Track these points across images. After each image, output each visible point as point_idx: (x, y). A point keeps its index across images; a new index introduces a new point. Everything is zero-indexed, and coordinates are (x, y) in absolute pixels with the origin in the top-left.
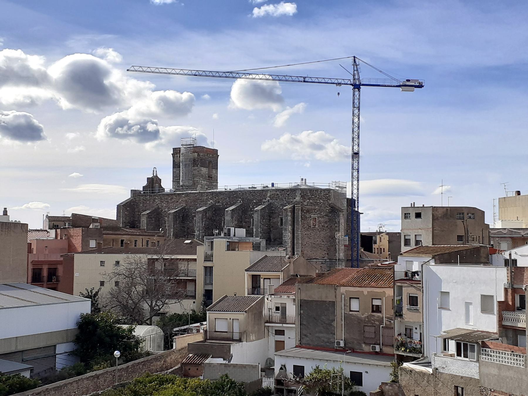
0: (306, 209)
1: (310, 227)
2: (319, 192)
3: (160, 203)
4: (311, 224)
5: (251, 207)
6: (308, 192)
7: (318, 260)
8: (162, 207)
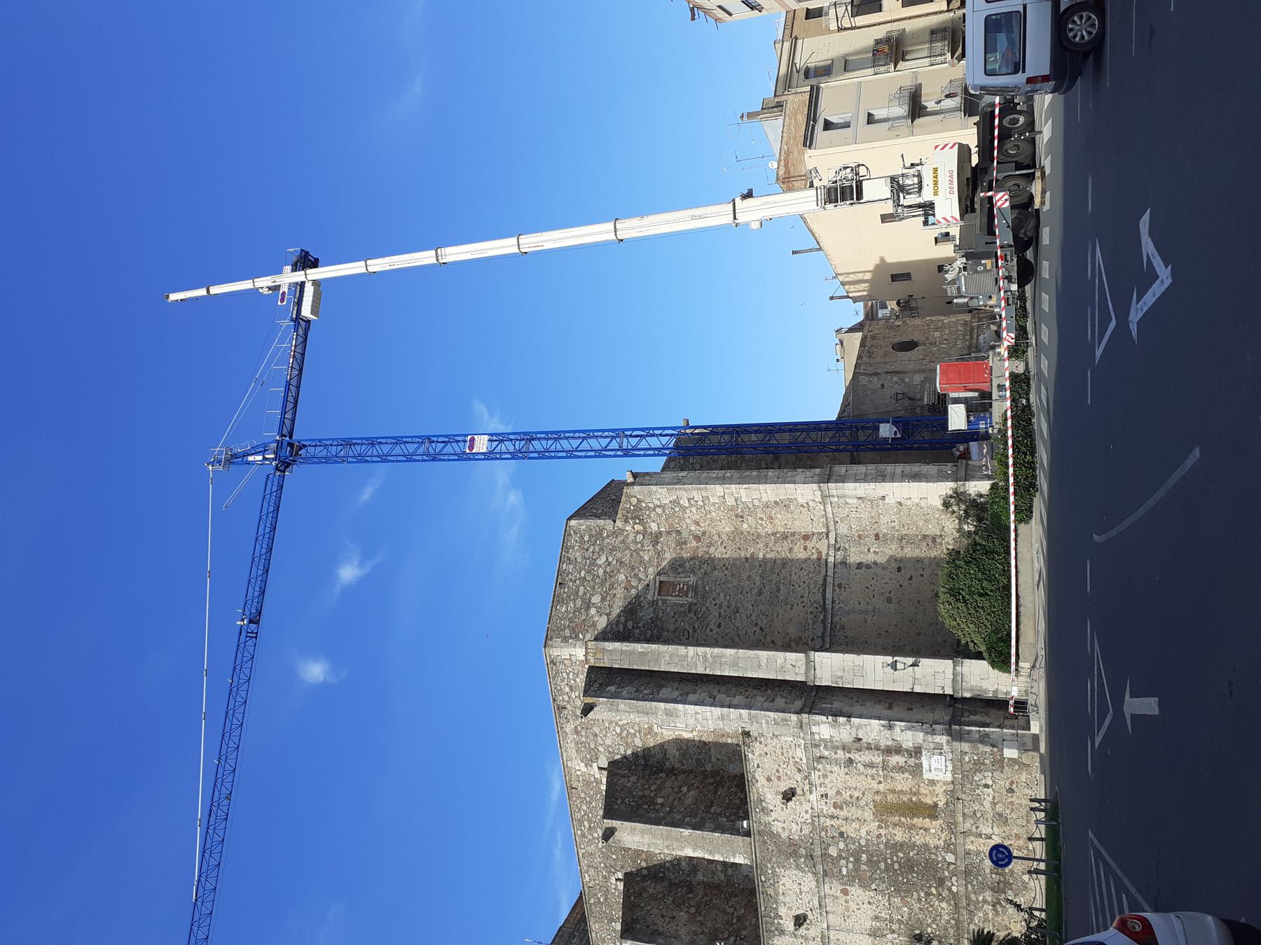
1: (691, 605)
2: (571, 567)
7: (830, 580)
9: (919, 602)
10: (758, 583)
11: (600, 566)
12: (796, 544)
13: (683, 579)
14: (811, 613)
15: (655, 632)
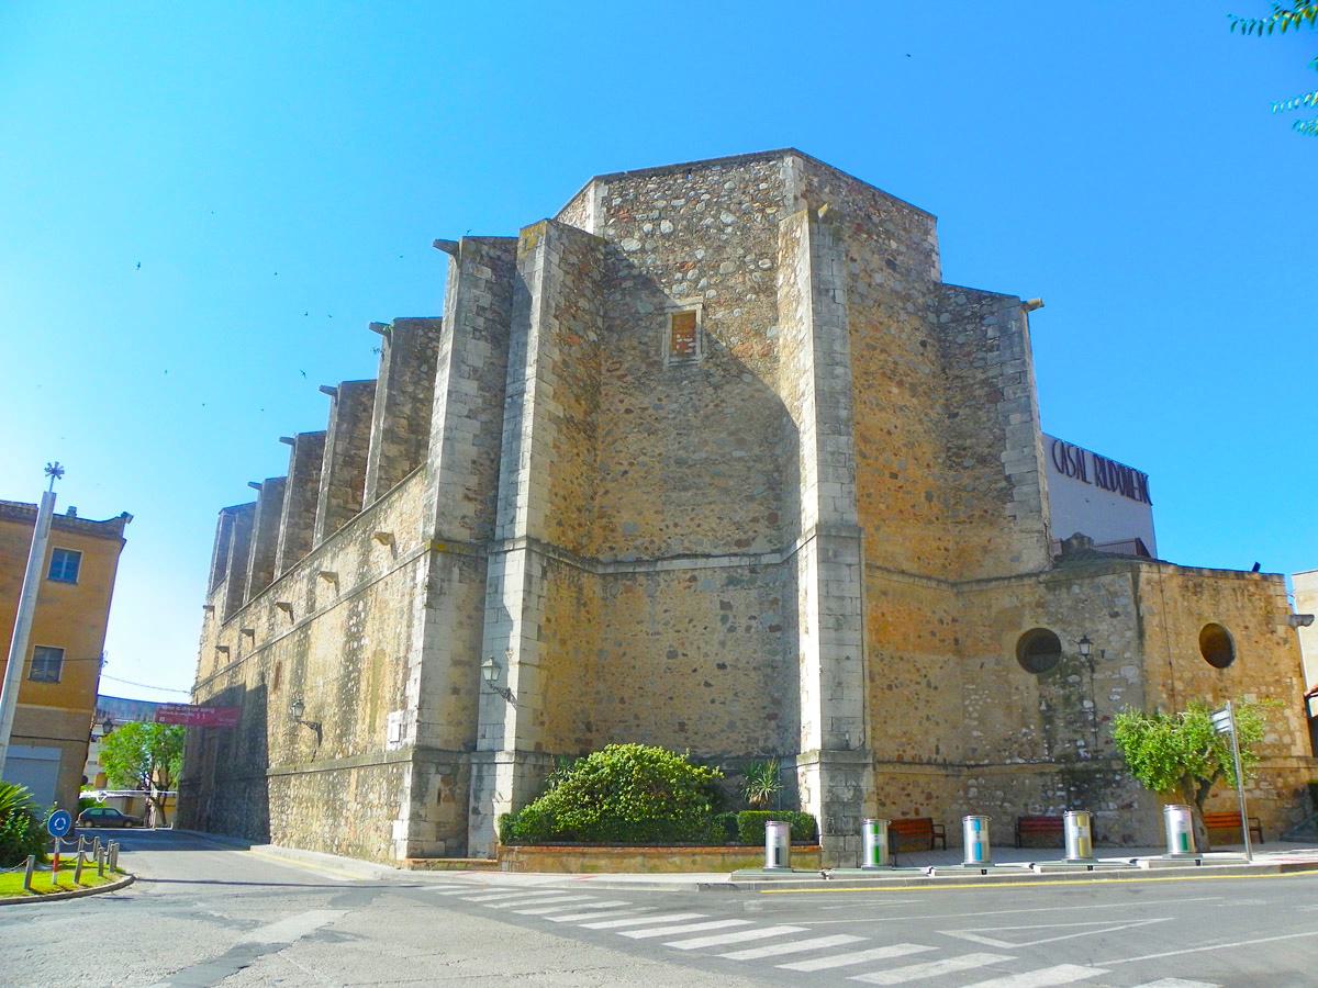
7: (701, 562)
9: (671, 698)
10: (696, 456)
12: (762, 504)
13: (698, 344)
14: (652, 542)
15: (618, 322)
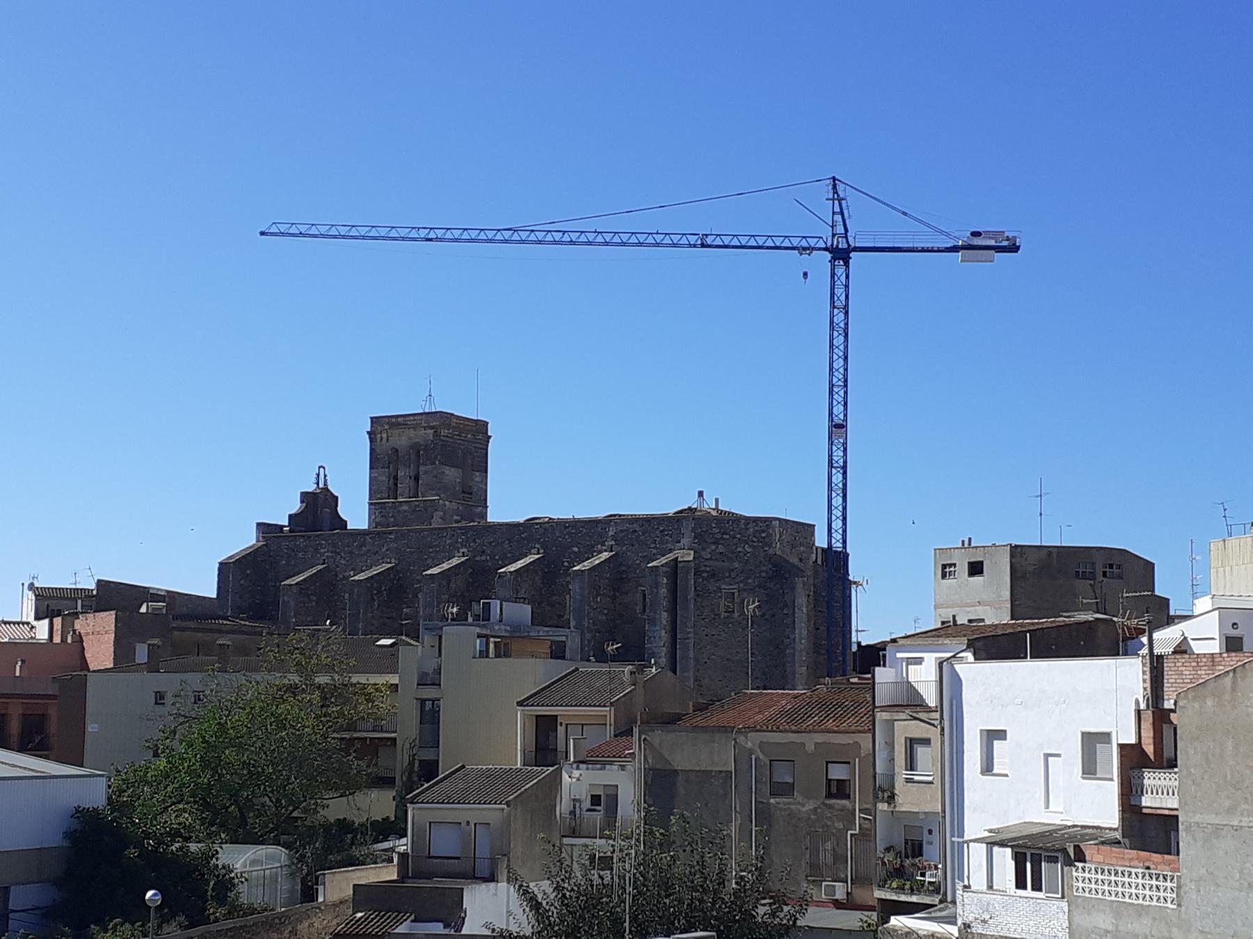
0: (708, 569)
1: (719, 615)
2: (743, 527)
3: (332, 557)
4: (722, 609)
5: (566, 564)
6: (714, 525)
8: (337, 566)
11: (744, 548)
